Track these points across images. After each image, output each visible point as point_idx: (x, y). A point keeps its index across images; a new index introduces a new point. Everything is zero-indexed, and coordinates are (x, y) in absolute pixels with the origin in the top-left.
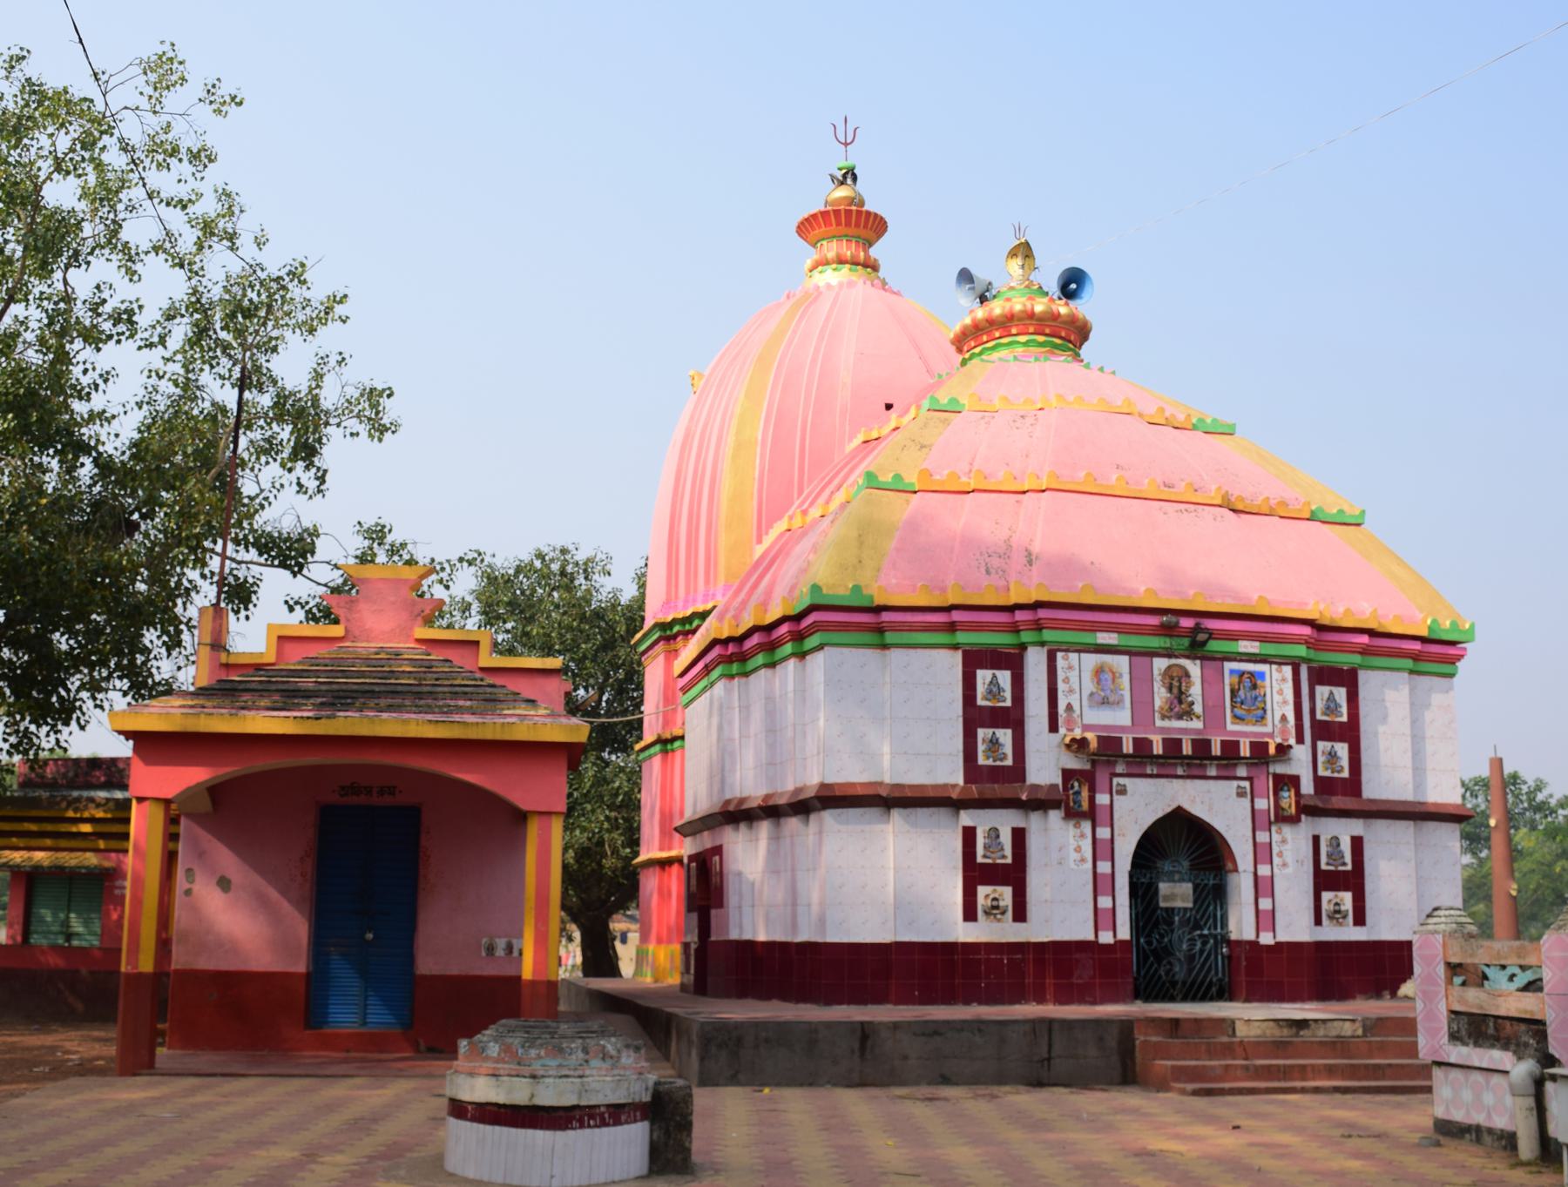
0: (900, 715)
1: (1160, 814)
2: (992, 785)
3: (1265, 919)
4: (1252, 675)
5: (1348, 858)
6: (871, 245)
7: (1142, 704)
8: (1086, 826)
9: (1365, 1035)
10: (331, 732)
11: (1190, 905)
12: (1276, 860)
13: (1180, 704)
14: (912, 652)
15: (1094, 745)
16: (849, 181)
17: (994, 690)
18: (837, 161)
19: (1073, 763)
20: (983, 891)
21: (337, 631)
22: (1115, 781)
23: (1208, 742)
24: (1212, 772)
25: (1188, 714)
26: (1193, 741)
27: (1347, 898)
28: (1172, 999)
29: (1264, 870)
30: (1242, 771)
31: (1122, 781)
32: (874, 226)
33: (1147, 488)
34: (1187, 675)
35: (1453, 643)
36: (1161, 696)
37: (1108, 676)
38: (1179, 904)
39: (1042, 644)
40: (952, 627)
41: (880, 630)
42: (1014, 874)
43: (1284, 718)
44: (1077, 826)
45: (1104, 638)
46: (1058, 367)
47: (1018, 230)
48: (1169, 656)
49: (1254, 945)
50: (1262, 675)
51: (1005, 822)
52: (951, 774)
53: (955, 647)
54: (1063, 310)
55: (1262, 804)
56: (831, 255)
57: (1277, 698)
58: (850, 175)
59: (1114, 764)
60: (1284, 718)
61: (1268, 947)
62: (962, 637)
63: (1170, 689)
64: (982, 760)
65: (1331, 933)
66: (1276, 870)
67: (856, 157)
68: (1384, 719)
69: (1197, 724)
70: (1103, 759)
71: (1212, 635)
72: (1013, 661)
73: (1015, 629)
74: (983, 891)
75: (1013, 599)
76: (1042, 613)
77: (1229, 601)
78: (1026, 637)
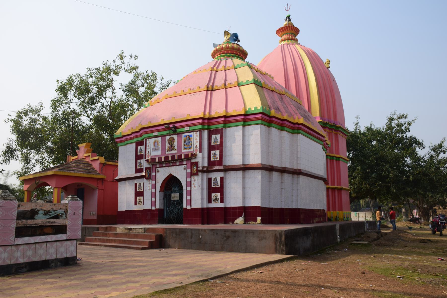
1: (166, 176)
3: (190, 202)
4: (189, 136)
5: (219, 184)
7: (163, 149)
8: (151, 181)
9: (144, 232)
11: (178, 199)
12: (192, 186)
13: (172, 148)
15: (150, 161)
16: (288, 20)
19: (148, 166)
21: (76, 157)
22: (157, 169)
23: (174, 156)
26: (171, 156)
27: (218, 195)
28: (173, 224)
30: (185, 163)
31: (158, 169)
33: (187, 91)
34: (174, 139)
36: (168, 145)
38: (176, 199)
40: (132, 138)
43: (196, 146)
44: (149, 181)
48: (170, 135)
49: (186, 209)
50: (191, 135)
57: (195, 141)
58: (288, 18)
59: (156, 165)
60: (196, 146)
62: (135, 140)
63: (170, 144)
65: (213, 205)
66: (192, 188)
68: (234, 141)
69: (175, 152)
71: (176, 128)
74: (138, 198)
77: (181, 118)
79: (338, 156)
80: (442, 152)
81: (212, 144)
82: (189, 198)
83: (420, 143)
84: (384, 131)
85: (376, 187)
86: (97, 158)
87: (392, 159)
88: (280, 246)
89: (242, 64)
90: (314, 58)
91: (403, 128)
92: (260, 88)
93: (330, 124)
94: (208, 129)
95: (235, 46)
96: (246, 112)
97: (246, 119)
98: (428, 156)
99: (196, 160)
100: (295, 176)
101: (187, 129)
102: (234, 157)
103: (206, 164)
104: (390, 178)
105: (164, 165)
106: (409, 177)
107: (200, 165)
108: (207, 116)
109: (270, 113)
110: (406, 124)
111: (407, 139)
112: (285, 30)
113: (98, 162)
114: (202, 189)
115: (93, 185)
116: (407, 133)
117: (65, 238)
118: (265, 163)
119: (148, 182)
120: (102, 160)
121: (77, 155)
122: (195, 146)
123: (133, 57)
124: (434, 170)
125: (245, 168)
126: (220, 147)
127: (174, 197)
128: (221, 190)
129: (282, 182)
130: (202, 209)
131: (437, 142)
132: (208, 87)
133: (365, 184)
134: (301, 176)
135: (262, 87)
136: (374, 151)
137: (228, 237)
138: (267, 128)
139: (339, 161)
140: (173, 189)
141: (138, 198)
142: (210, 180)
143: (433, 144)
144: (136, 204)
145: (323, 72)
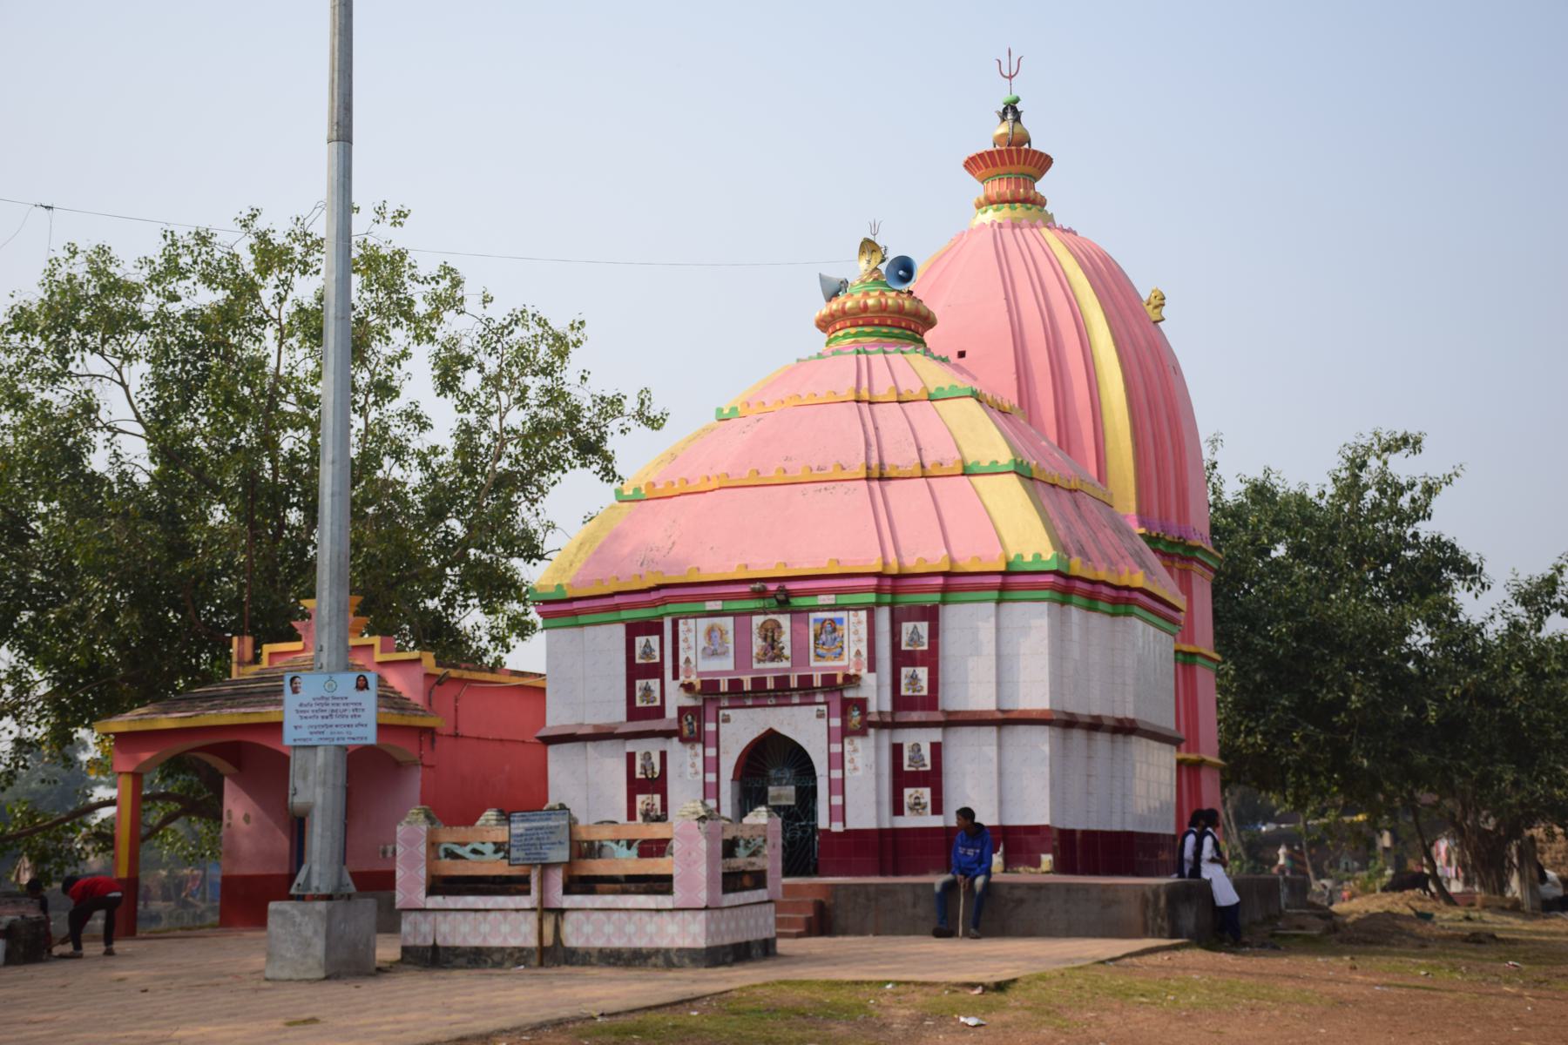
1: (756, 735)
3: (839, 813)
4: (832, 621)
5: (928, 761)
6: (1036, 180)
7: (742, 655)
8: (699, 747)
11: (792, 803)
12: (847, 765)
13: (773, 650)
14: (598, 628)
15: (698, 687)
16: (1010, 116)
17: (648, 650)
19: (689, 702)
20: (908, 793)
21: (297, 646)
23: (787, 678)
24: (796, 700)
25: (779, 657)
27: (926, 794)
30: (820, 698)
31: (727, 712)
34: (779, 627)
36: (758, 644)
37: (717, 634)
38: (784, 802)
39: (668, 614)
40: (617, 608)
43: (858, 653)
44: (692, 748)
47: (875, 227)
49: (827, 832)
50: (841, 621)
51: (654, 747)
52: (616, 714)
53: (621, 621)
57: (853, 637)
58: (1011, 111)
59: (718, 700)
60: (858, 653)
61: (838, 834)
62: (625, 615)
63: (765, 639)
65: (908, 821)
66: (847, 773)
67: (1019, 88)
69: (786, 664)
70: (712, 696)
71: (789, 594)
74: (640, 798)
77: (806, 566)
79: (1192, 649)
80: (1555, 606)
81: (904, 647)
83: (1472, 569)
84: (1323, 503)
85: (1296, 746)
86: (416, 654)
87: (1360, 636)
88: (1155, 920)
89: (952, 387)
90: (1110, 281)
91: (1404, 502)
92: (1028, 483)
93: (1168, 538)
94: (892, 605)
95: (907, 304)
96: (1008, 564)
97: (1007, 583)
98: (1501, 625)
99: (861, 694)
100: (1120, 737)
101: (823, 600)
102: (972, 688)
103: (887, 706)
104: (1350, 713)
105: (749, 702)
106: (1424, 707)
107: (872, 707)
108: (894, 569)
109: (1068, 567)
110: (1418, 488)
111: (1417, 546)
112: (1003, 164)
113: (417, 673)
114: (878, 776)
115: (405, 749)
116: (1419, 524)
117: (670, 906)
118: (1055, 707)
120: (429, 660)
121: (299, 638)
122: (853, 653)
123: (389, 215)
124: (1523, 683)
125: (1004, 721)
126: (931, 659)
127: (779, 797)
128: (933, 779)
129: (1089, 757)
130: (881, 833)
131: (1540, 569)
132: (868, 468)
133: (1250, 732)
134: (1134, 738)
135: (1031, 479)
136: (1290, 601)
138: (1056, 606)
139: (1193, 665)
140: (772, 772)
141: (640, 798)
142: (897, 750)
143: (1523, 577)
145: (1143, 343)
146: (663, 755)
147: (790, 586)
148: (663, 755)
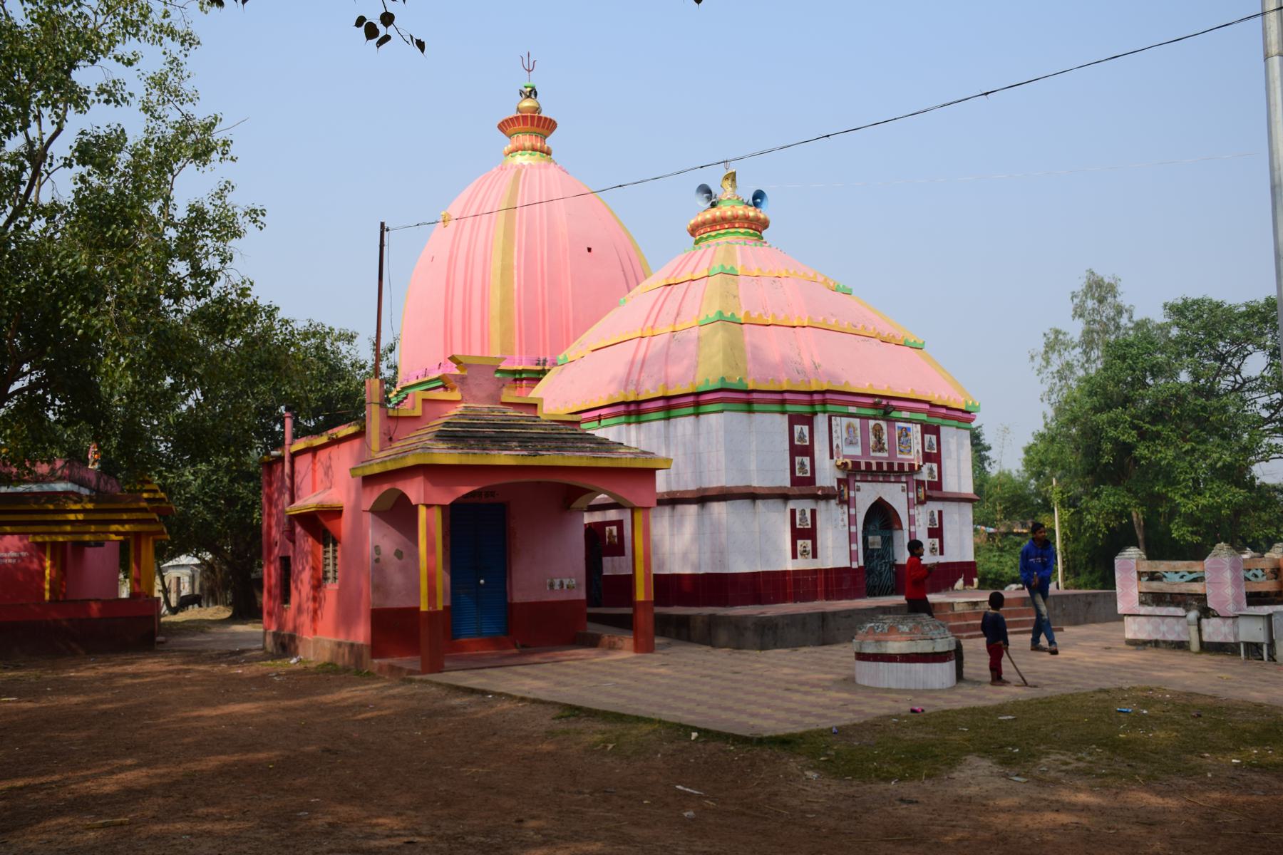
0: (760, 449)
2: (803, 486)
4: (907, 430)
10: (542, 463)
15: (850, 466)
18: (524, 82)
19: (840, 475)
25: (882, 450)
29: (913, 529)
30: (904, 479)
32: (547, 126)
33: (846, 325)
35: (969, 413)
36: (872, 439)
39: (824, 412)
41: (749, 403)
42: (811, 534)
45: (852, 410)
46: (753, 248)
51: (807, 505)
53: (783, 413)
54: (752, 214)
55: (911, 495)
56: (528, 144)
58: (533, 93)
62: (789, 408)
64: (798, 474)
67: (535, 81)
69: (885, 455)
71: (895, 409)
72: (809, 420)
73: (812, 403)
74: (800, 542)
75: (814, 388)
76: (828, 396)
78: (818, 408)
82: (854, 547)
101: (905, 414)
119: (840, 510)
127: (873, 544)
137: (1090, 604)
141: (800, 542)
144: (794, 556)
146: (813, 512)
147: (894, 403)
148: (813, 512)
